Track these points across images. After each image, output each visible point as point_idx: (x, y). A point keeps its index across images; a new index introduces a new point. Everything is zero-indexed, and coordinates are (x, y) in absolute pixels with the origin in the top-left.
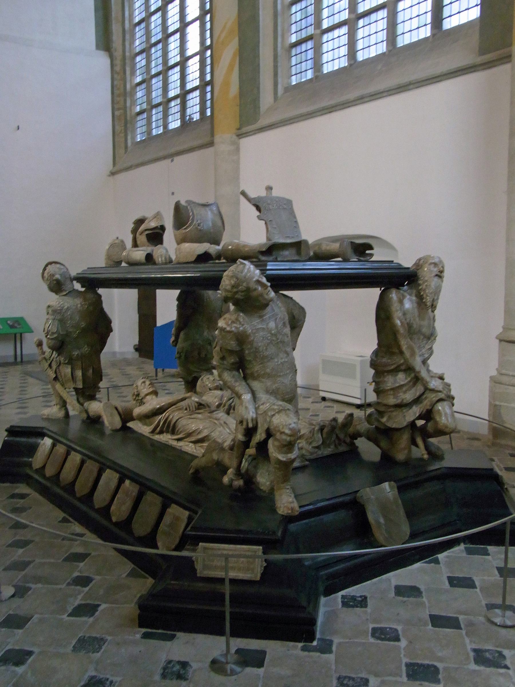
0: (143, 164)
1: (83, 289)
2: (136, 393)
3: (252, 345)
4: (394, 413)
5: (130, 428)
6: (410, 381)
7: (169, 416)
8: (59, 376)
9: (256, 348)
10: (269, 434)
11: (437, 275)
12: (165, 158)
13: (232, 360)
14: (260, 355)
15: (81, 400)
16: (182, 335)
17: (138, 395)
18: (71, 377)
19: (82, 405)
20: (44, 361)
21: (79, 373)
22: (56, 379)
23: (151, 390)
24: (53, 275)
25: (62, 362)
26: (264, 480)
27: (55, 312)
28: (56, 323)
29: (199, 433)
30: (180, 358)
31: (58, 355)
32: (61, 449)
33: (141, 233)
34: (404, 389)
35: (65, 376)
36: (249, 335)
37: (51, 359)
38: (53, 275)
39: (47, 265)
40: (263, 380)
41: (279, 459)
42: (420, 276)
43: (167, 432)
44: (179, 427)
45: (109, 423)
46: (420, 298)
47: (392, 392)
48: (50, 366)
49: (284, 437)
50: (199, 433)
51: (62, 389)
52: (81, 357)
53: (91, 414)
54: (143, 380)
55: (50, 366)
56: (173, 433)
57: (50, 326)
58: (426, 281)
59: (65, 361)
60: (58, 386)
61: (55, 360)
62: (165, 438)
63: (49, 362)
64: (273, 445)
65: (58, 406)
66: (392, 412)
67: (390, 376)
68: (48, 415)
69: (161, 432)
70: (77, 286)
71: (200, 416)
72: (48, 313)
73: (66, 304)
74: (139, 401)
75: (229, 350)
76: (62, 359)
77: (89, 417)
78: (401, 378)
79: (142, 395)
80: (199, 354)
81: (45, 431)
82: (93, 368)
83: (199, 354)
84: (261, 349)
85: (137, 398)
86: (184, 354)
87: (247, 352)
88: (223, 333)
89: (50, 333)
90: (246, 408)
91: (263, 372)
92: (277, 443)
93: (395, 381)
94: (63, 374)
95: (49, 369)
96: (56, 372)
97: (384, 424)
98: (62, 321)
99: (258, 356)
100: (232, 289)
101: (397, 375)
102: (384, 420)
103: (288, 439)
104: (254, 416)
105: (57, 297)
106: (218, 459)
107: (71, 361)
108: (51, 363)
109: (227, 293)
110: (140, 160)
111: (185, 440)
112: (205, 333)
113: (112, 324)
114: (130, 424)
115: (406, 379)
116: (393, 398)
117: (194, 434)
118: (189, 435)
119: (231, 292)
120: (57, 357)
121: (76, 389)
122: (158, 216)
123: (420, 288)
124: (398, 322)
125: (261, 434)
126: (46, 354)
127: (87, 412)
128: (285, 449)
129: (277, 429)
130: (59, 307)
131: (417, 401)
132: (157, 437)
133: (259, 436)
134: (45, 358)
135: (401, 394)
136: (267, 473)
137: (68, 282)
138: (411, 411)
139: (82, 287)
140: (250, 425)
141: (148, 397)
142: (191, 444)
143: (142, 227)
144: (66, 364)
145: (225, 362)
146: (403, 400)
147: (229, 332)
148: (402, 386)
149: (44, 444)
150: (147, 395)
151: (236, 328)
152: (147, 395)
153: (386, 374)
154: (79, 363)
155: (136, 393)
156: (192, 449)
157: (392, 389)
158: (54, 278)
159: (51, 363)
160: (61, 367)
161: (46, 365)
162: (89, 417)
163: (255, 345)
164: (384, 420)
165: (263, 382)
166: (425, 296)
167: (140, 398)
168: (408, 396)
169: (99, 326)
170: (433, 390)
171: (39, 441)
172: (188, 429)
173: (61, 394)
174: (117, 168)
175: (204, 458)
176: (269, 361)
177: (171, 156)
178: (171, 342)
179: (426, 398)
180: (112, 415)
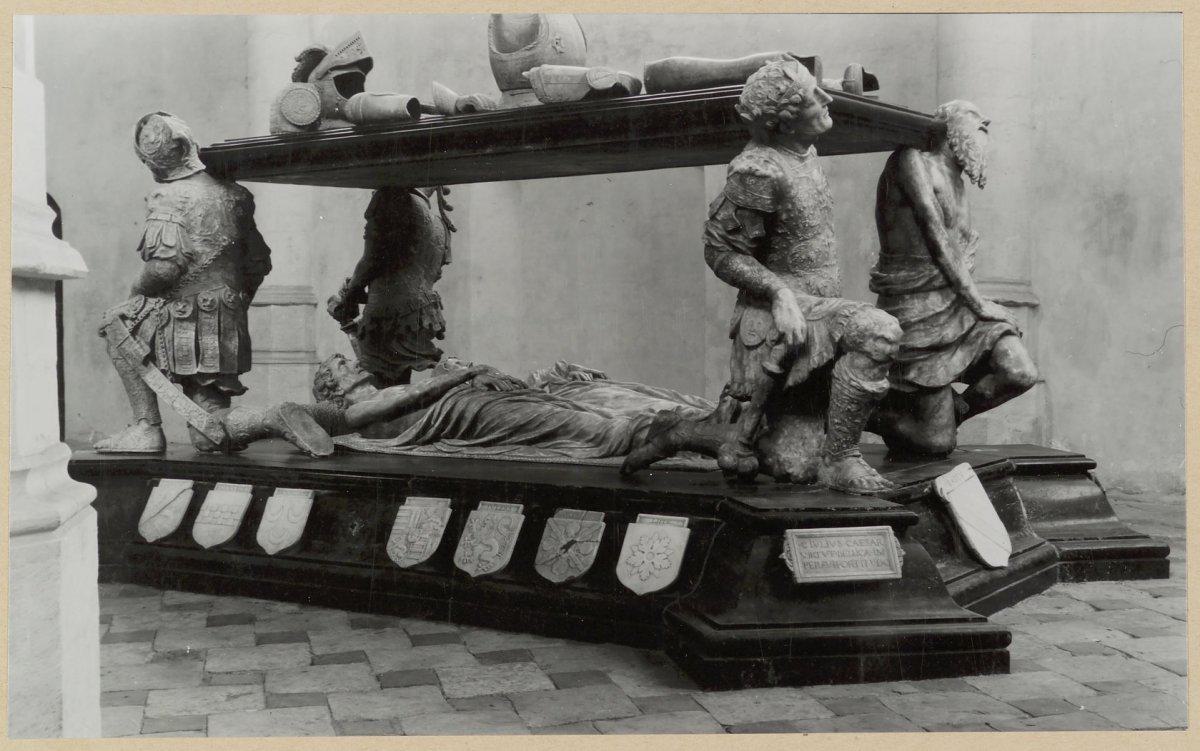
4: (928, 363)
6: (949, 308)
7: (452, 409)
8: (160, 352)
9: (800, 212)
10: (840, 349)
11: (981, 129)
18: (193, 349)
20: (120, 321)
21: (211, 342)
22: (151, 359)
34: (943, 319)
36: (791, 187)
37: (142, 314)
41: (865, 391)
46: (957, 166)
47: (922, 326)
49: (880, 345)
52: (218, 308)
55: (134, 332)
58: (967, 137)
64: (852, 366)
67: (916, 301)
78: (936, 302)
84: (806, 213)
87: (784, 216)
88: (750, 181)
92: (862, 361)
93: (925, 309)
95: (132, 339)
96: (152, 344)
97: (911, 384)
101: (926, 298)
102: (912, 375)
103: (888, 348)
104: (805, 326)
115: (943, 302)
116: (926, 336)
119: (775, 104)
120: (161, 308)
123: (956, 149)
127: (224, 427)
128: (876, 371)
129: (867, 333)
131: (963, 340)
133: (817, 357)
140: (801, 338)
145: (740, 238)
147: (764, 177)
148: (939, 314)
151: (775, 171)
153: (907, 297)
154: (214, 321)
157: (922, 321)
160: (168, 331)
164: (912, 375)
166: (967, 161)
168: (951, 332)
170: (991, 320)
176: (814, 237)
179: (979, 335)
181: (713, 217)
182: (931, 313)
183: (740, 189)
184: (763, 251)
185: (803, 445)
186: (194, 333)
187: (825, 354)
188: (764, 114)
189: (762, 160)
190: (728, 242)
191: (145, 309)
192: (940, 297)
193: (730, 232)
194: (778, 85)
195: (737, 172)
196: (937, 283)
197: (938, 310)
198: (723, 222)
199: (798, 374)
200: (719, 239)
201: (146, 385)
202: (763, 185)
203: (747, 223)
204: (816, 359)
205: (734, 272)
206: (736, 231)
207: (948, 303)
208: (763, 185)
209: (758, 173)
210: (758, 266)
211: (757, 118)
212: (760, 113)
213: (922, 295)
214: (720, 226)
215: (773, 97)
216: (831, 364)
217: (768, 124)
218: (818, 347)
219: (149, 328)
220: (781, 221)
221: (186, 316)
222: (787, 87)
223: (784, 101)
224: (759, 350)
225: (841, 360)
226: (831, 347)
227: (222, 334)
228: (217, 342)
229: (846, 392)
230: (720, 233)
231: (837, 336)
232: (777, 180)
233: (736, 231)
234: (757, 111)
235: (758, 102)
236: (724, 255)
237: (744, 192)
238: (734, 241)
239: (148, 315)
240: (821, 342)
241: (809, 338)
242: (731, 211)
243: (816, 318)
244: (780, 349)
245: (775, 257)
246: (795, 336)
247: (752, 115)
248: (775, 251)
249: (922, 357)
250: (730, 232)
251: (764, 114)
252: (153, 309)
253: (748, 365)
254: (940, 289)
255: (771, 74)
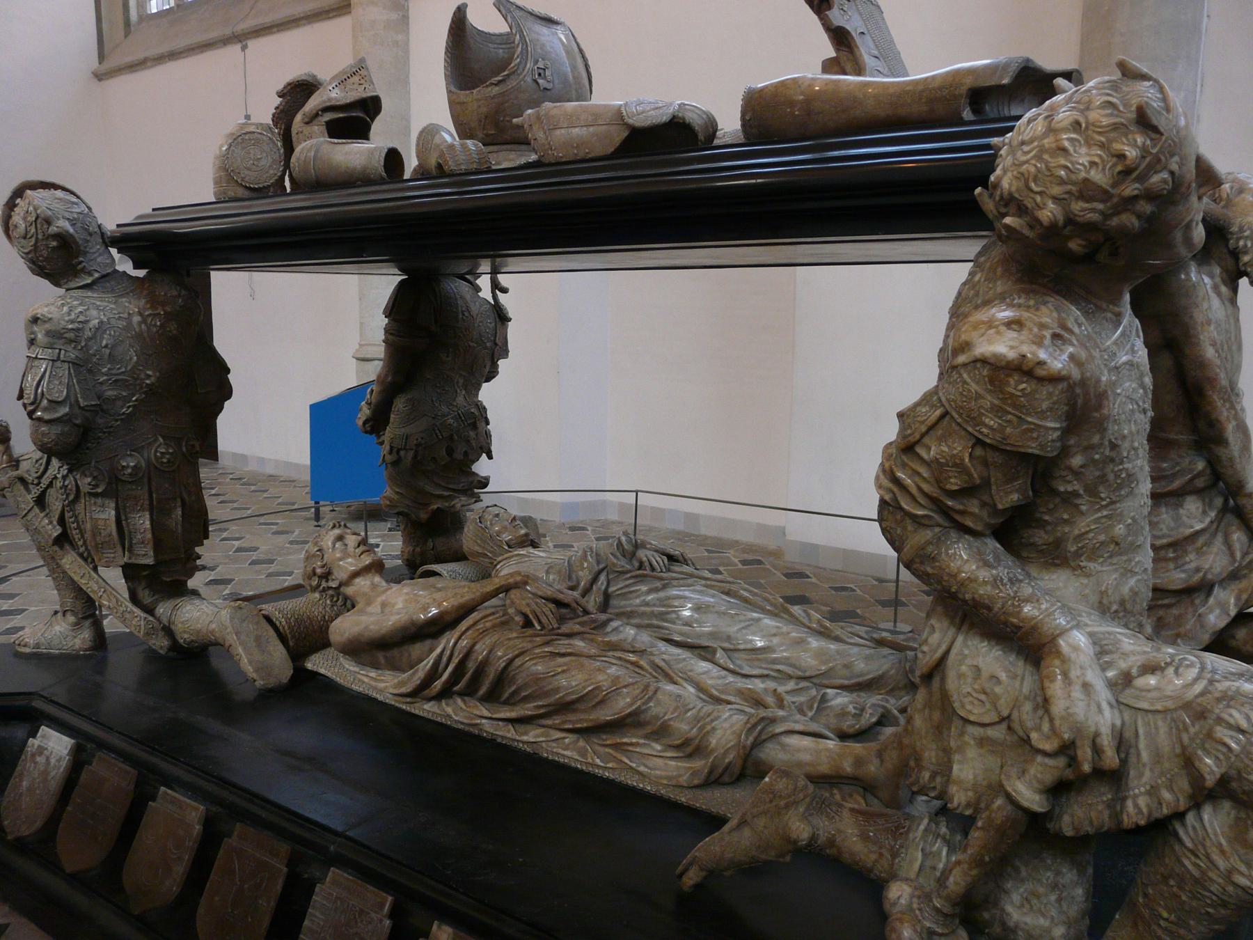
0: (173, 55)
1: (141, 273)
2: (319, 571)
3: (1102, 431)
4: (1175, 611)
5: (315, 674)
8: (75, 534)
12: (225, 41)
13: (1010, 498)
14: (1117, 476)
15: (146, 597)
16: (400, 404)
17: (327, 576)
18: (114, 533)
19: (150, 611)
21: (142, 522)
22: (63, 540)
23: (367, 560)
24: (48, 222)
25: (85, 489)
26: (1043, 922)
27: (56, 335)
28: (64, 371)
29: (602, 702)
30: (395, 463)
31: (70, 471)
32: (111, 775)
33: (311, 119)
34: (1201, 541)
35: (96, 532)
37: (45, 481)
38: (48, 222)
39: (19, 193)
40: (1091, 565)
42: (1235, 229)
43: (469, 692)
44: (520, 681)
45: (256, 671)
48: (41, 501)
50: (602, 702)
51: (88, 569)
53: (183, 637)
54: (337, 531)
55: (41, 501)
56: (492, 697)
57: (45, 382)
59: (96, 486)
60: (70, 561)
61: (59, 484)
62: (457, 712)
63: (35, 491)
65: (71, 619)
66: (1169, 606)
68: (37, 646)
69: (445, 694)
70: (125, 265)
71: (579, 644)
72: (32, 342)
73: (94, 313)
74: (330, 592)
75: (1025, 457)
76: (85, 482)
77: (175, 645)
79: (340, 575)
80: (450, 451)
81: (38, 704)
82: (183, 504)
83: (450, 451)
85: (324, 584)
86: (411, 454)
87: (1077, 461)
88: (1018, 386)
89: (45, 402)
90: (1086, 686)
91: (1102, 538)
94: (88, 526)
95: (36, 510)
96: (62, 521)
98: (83, 367)
99: (1111, 477)
100: (1115, 185)
105: (62, 291)
106: (813, 838)
107: (115, 488)
108: (43, 493)
109: (1077, 206)
110: (164, 48)
111: (549, 722)
112: (460, 400)
113: (231, 377)
114: (317, 663)
115: (1204, 513)
117: (580, 706)
118: (565, 707)
119: (1105, 195)
120: (64, 477)
121: (130, 572)
122: (363, 72)
124: (1210, 353)
125: (1153, 791)
126: (24, 466)
127: (168, 631)
130: (72, 322)
132: (427, 709)
134: (22, 480)
135: (1192, 556)
136: (1053, 898)
137: (96, 246)
138: (1211, 600)
139: (137, 266)
141: (357, 580)
142: (569, 739)
143: (313, 103)
144: (96, 495)
145: (974, 506)
146: (1205, 574)
147: (1055, 379)
148: (1197, 534)
149: (41, 750)
150: (356, 574)
152: (356, 574)
154: (142, 493)
155: (319, 571)
156: (583, 753)
158: (53, 230)
159: (43, 493)
160: (80, 507)
161: (29, 498)
162: (175, 645)
163: (1112, 428)
165: (1088, 576)
167: (334, 584)
169: (193, 382)
171: (20, 731)
172: (557, 690)
173: (82, 582)
174: (110, 64)
175: (747, 832)
177: (240, 38)
178: (360, 423)
180: (258, 639)
181: (906, 448)
182: (1188, 531)
183: (989, 400)
184: (1010, 533)
185: (1059, 900)
186: (113, 513)
187: (1167, 795)
188: (1070, 221)
189: (1048, 334)
190: (945, 512)
191: (49, 472)
192: (1199, 504)
193: (952, 494)
194: (1117, 146)
195: (983, 361)
196: (1200, 483)
197: (1198, 527)
198: (938, 467)
199: (1085, 813)
200: (922, 500)
201: (64, 572)
202: (1046, 397)
203: (996, 476)
204: (1142, 802)
205: (955, 576)
206: (968, 491)
207: (1213, 514)
208: (1046, 397)
209: (1040, 372)
210: (1006, 568)
211: (1052, 230)
212: (1061, 218)
213: (1173, 500)
214: (925, 472)
215: (1096, 176)
216: (1180, 816)
217: (1075, 245)
218: (1148, 774)
219: (56, 502)
220: (1070, 468)
221: (99, 490)
222: (1145, 151)
223: (1130, 189)
224: (990, 732)
225: (1207, 813)
226: (1184, 784)
227: (158, 512)
228: (148, 523)
229: (1214, 888)
230: (925, 487)
231: (1210, 765)
232: (1083, 382)
233: (968, 491)
234: (1049, 212)
235: (1056, 190)
236: (928, 534)
237: (998, 411)
238: (962, 513)
239: (50, 485)
240: (1157, 757)
241: (1123, 743)
242: (958, 448)
243: (1145, 705)
244: (1046, 770)
245: (1041, 537)
246: (1097, 750)
247: (1035, 223)
248: (1042, 524)
249: (1166, 601)
250: (952, 494)
251: (1070, 221)
252: (56, 478)
253: (960, 749)
254: (1199, 492)
255: (1093, 115)
